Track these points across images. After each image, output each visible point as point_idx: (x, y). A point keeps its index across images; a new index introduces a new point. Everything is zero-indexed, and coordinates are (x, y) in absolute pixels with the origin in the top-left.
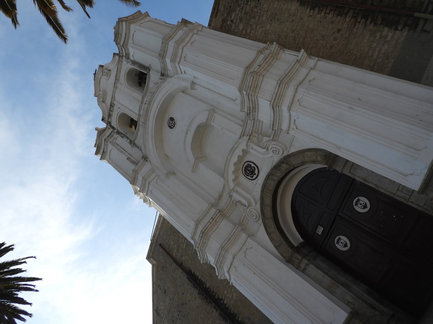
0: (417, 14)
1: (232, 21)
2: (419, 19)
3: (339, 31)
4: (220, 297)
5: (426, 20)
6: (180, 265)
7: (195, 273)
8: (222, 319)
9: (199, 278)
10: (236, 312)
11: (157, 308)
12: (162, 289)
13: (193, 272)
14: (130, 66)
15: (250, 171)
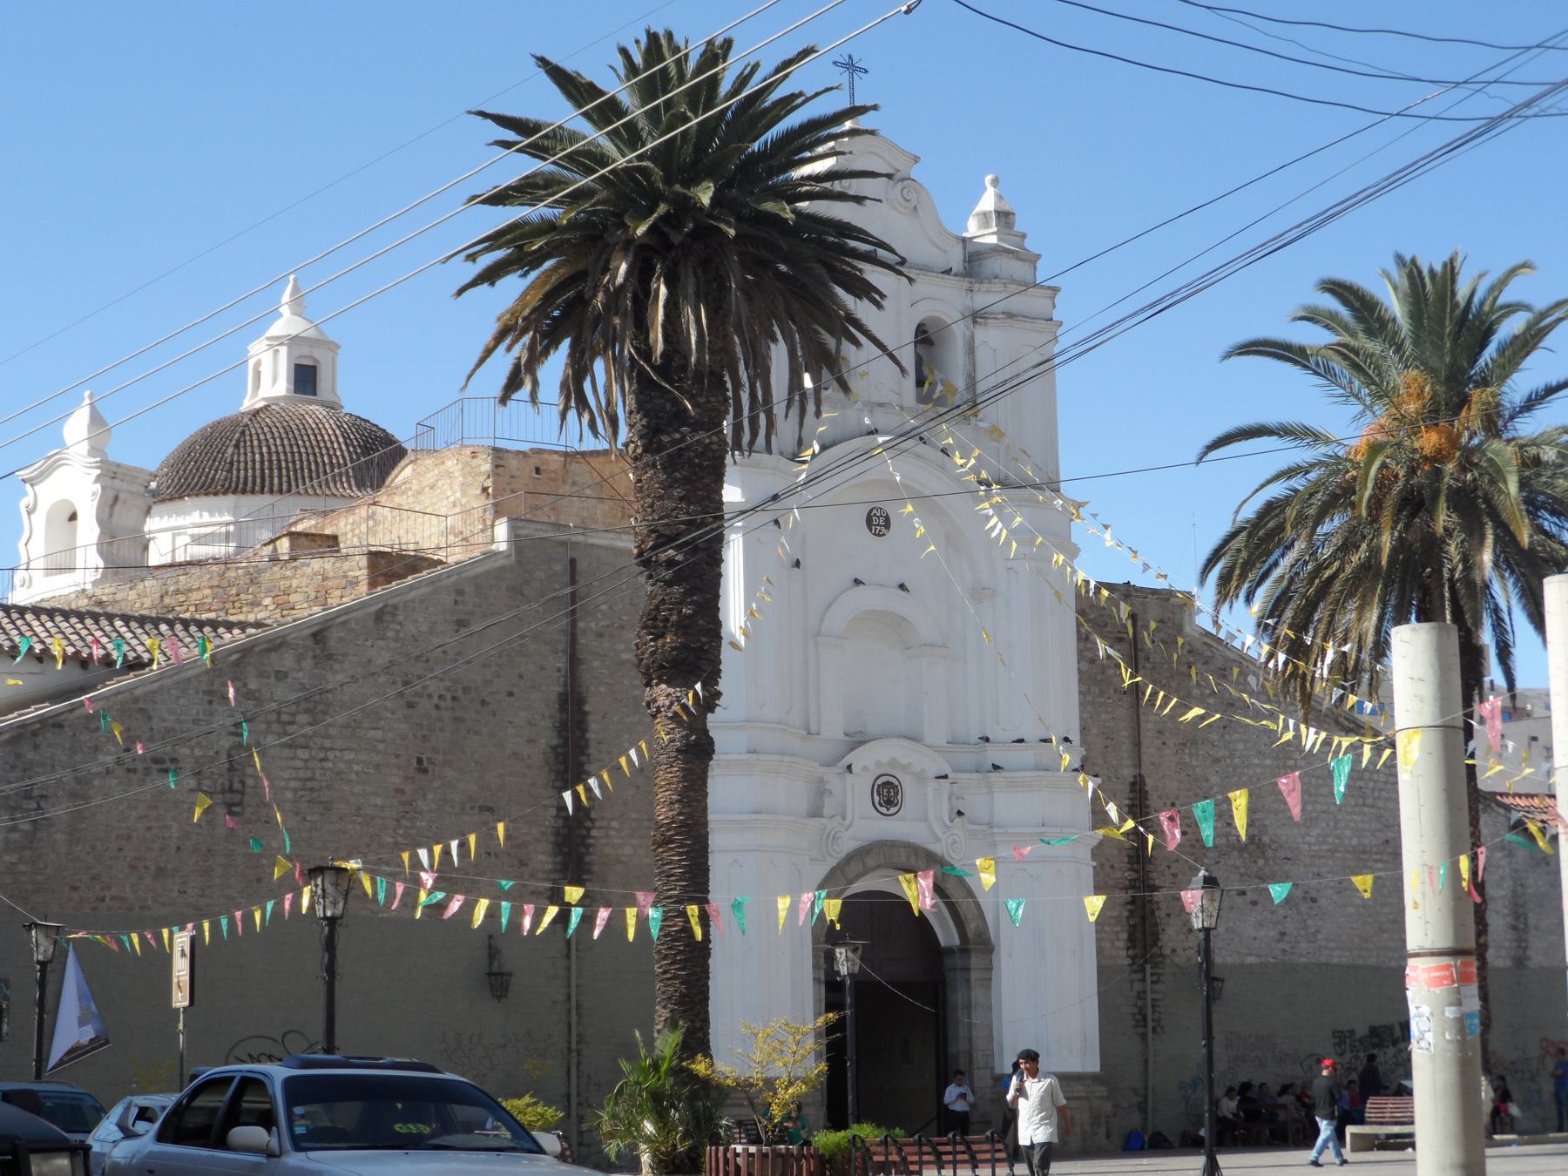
0: (1148, 967)
1: (1087, 639)
2: (1143, 970)
3: (1112, 867)
4: (593, 815)
5: (1143, 980)
6: (574, 661)
7: (590, 718)
8: (552, 839)
9: (588, 735)
10: (595, 868)
11: (395, 607)
12: (460, 607)
13: (587, 708)
14: (959, 331)
15: (887, 795)
